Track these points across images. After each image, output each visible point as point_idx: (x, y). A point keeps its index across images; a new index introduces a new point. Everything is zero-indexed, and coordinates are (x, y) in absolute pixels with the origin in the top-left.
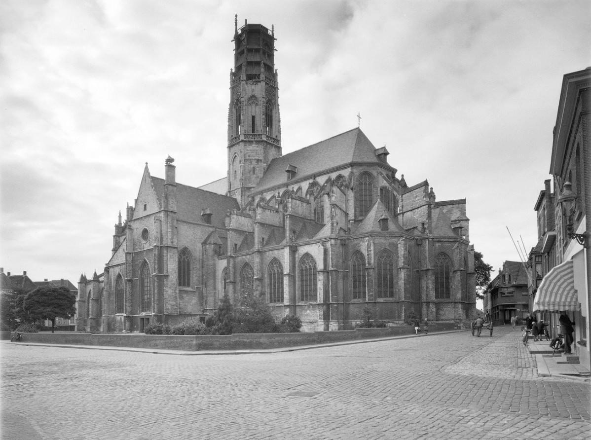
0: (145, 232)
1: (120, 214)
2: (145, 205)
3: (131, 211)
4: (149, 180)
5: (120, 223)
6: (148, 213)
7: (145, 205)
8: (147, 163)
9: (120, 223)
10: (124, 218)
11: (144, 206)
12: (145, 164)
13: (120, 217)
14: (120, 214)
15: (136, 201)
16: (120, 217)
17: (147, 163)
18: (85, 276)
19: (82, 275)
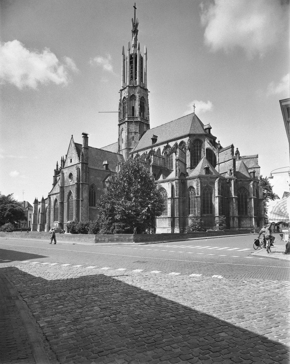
0: (71, 175)
1: (57, 163)
2: (71, 160)
3: (63, 162)
4: (73, 145)
5: (57, 169)
6: (73, 163)
7: (71, 160)
8: (72, 136)
9: (57, 169)
10: (60, 166)
11: (70, 160)
12: (71, 136)
13: (57, 165)
14: (57, 163)
15: (66, 156)
16: (57, 165)
17: (72, 136)
18: (37, 199)
19: (36, 199)
